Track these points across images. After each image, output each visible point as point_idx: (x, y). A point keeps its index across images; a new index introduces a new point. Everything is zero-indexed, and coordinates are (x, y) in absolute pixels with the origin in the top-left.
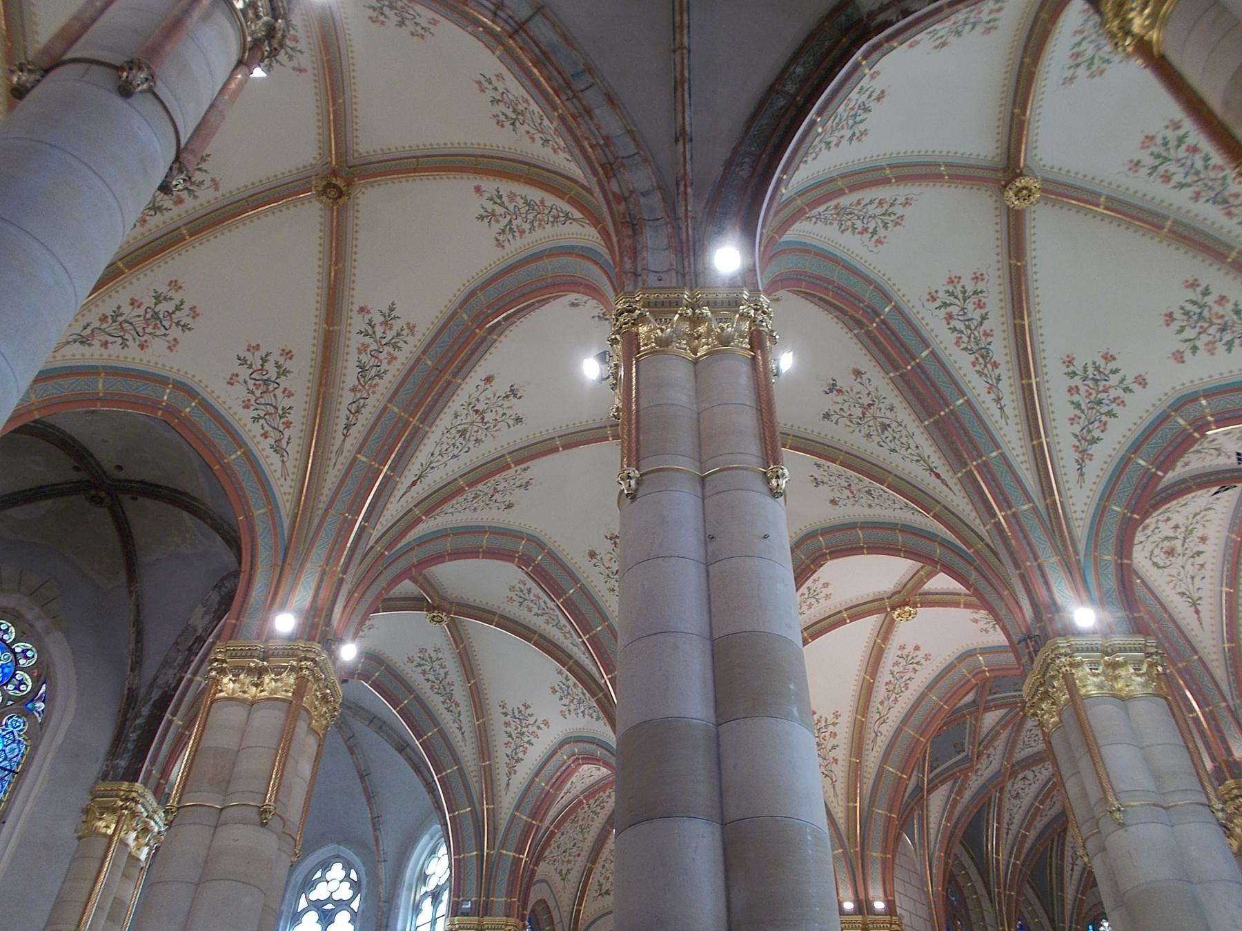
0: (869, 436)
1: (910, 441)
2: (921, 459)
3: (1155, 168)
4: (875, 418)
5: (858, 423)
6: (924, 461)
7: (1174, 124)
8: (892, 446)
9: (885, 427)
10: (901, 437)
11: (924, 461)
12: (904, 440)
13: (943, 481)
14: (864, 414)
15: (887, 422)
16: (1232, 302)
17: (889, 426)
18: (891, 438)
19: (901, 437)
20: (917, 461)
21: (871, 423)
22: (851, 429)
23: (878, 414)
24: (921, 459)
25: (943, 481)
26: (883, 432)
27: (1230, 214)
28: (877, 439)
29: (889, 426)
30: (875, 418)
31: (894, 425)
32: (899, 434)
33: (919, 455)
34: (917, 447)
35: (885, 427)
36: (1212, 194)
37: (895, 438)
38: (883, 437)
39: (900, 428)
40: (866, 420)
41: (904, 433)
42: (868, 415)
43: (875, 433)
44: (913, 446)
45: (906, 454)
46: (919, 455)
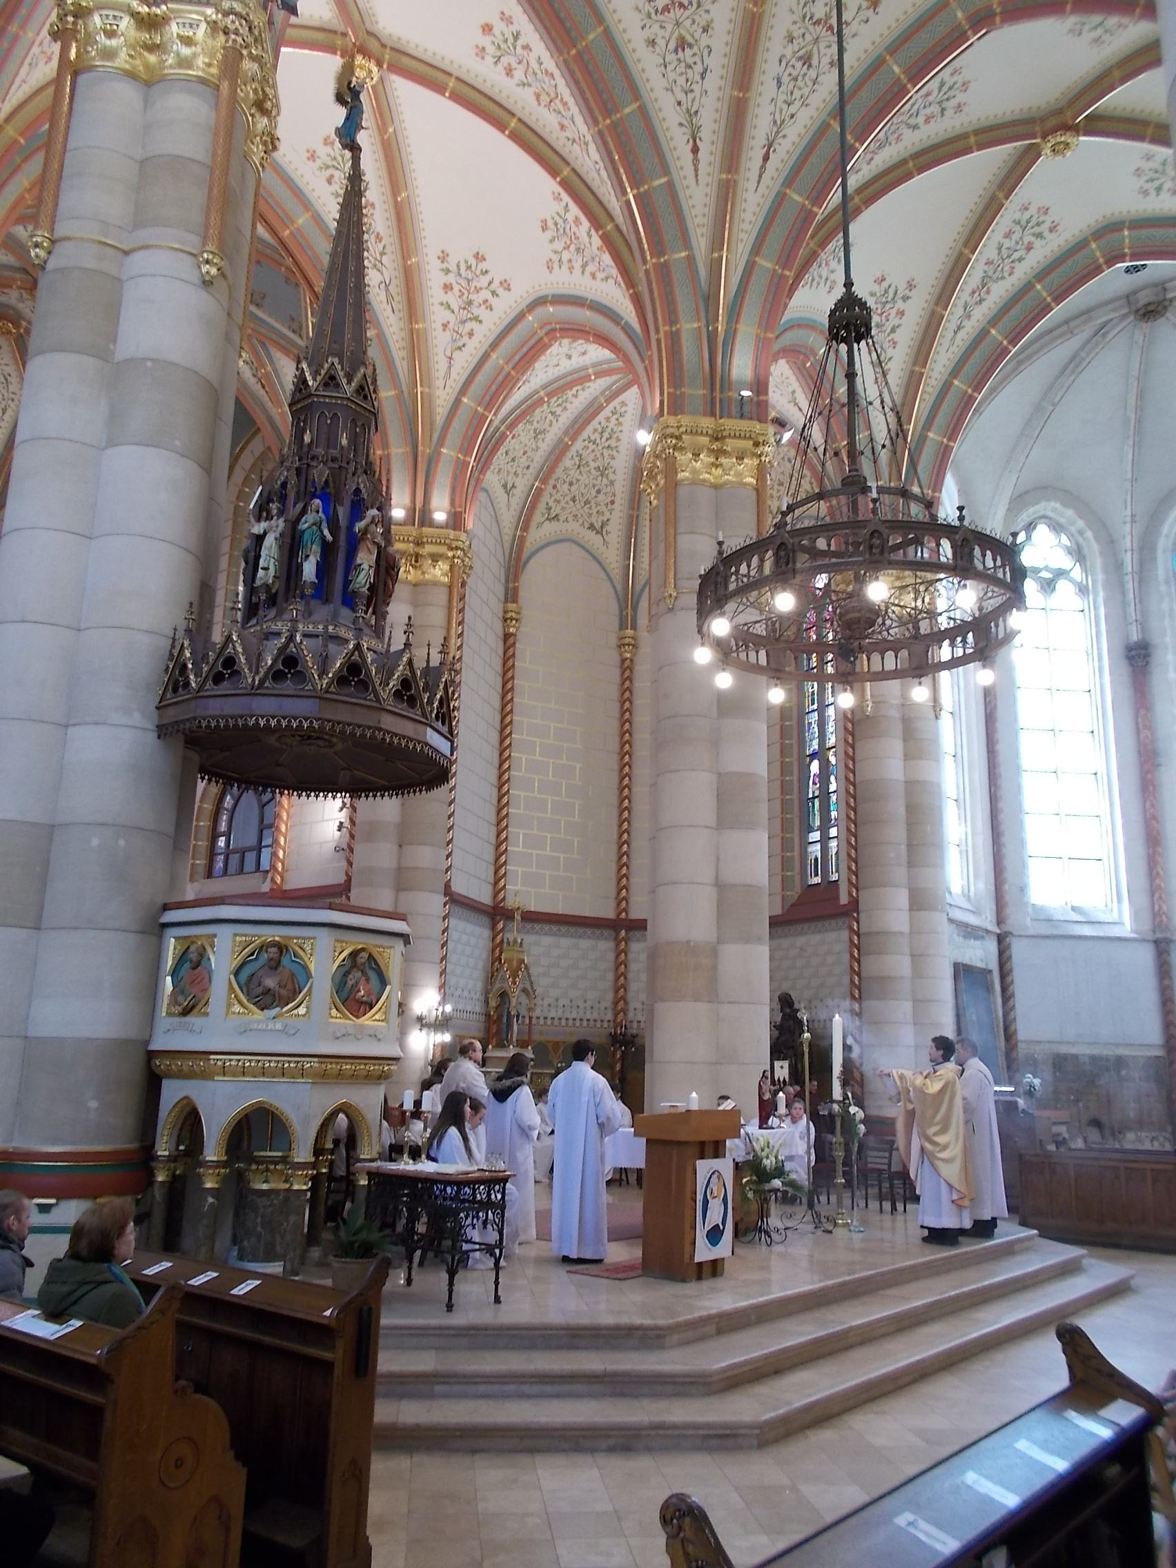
0: (791, 39)
1: (798, 104)
2: (779, 126)
3: (1019, 223)
4: (816, 40)
5: (804, 17)
6: (777, 132)
7: (1055, 227)
8: (785, 79)
9: (807, 60)
10: (800, 89)
11: (777, 132)
12: (797, 94)
13: (763, 169)
14: (818, 22)
15: (815, 62)
16: (900, 322)
17: (810, 66)
18: (795, 73)
19: (800, 89)
20: (775, 122)
21: (808, 38)
22: (794, 8)
23: (822, 45)
24: (779, 126)
25: (763, 169)
26: (800, 58)
27: (974, 292)
28: (788, 52)
29: (810, 66)
30: (816, 40)
31: (812, 73)
32: (802, 85)
33: (783, 122)
34: (792, 116)
35: (807, 60)
36: (990, 274)
37: (796, 79)
38: (793, 61)
39: (810, 84)
40: (811, 28)
41: (806, 91)
42: (818, 28)
43: (796, 48)
44: (793, 109)
45: (780, 103)
46: (783, 122)
